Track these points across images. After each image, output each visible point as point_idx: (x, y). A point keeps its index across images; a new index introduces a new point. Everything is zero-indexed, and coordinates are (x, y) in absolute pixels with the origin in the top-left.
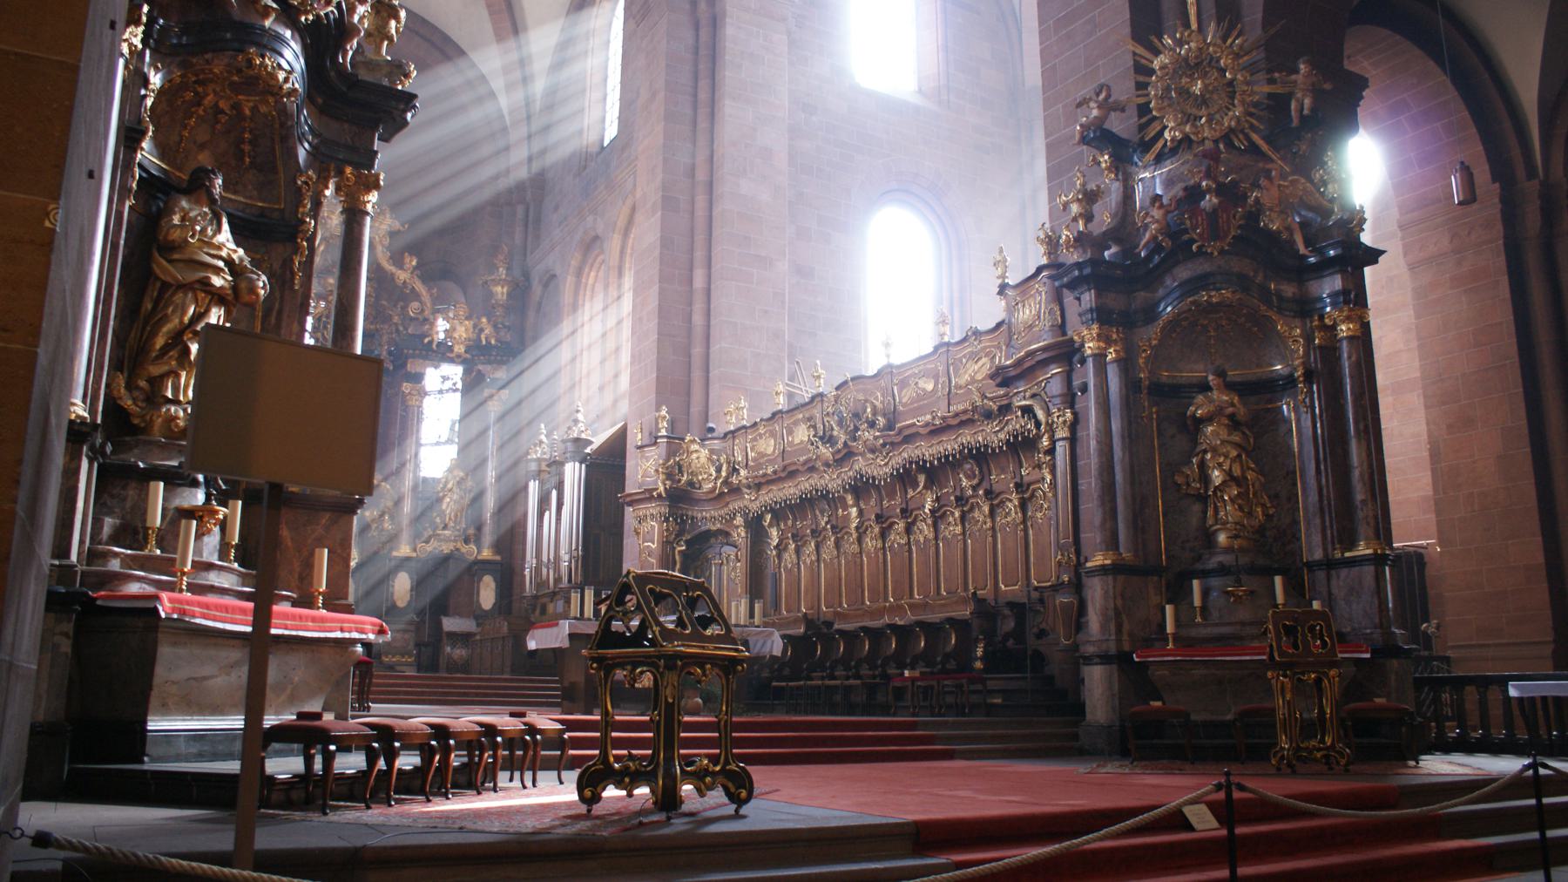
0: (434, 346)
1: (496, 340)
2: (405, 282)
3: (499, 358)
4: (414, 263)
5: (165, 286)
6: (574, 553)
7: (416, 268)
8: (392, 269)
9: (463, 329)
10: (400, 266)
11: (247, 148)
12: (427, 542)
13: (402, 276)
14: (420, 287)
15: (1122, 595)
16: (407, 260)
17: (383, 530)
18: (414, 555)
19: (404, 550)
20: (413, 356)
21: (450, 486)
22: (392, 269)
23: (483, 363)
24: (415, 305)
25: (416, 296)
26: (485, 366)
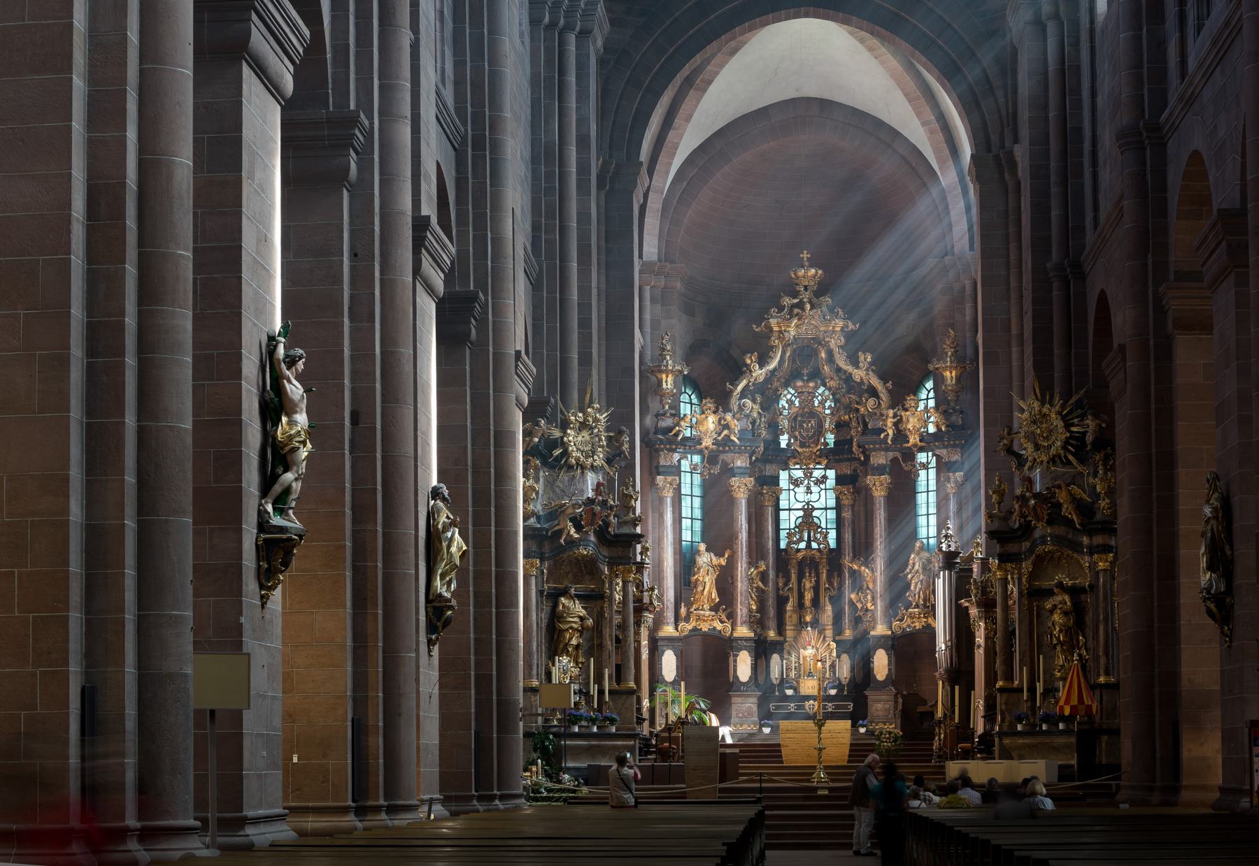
0: (889, 442)
1: (947, 426)
2: (861, 379)
3: (952, 443)
4: (869, 359)
5: (560, 630)
6: (949, 644)
7: (871, 364)
8: (850, 369)
9: (916, 420)
10: (856, 364)
11: (583, 568)
12: (901, 620)
13: (858, 374)
14: (875, 382)
15: (1006, 704)
16: (862, 358)
17: (867, 610)
18: (890, 633)
19: (880, 629)
20: (875, 450)
21: (917, 567)
22: (850, 369)
23: (939, 448)
24: (871, 402)
25: (873, 392)
26: (942, 451)
